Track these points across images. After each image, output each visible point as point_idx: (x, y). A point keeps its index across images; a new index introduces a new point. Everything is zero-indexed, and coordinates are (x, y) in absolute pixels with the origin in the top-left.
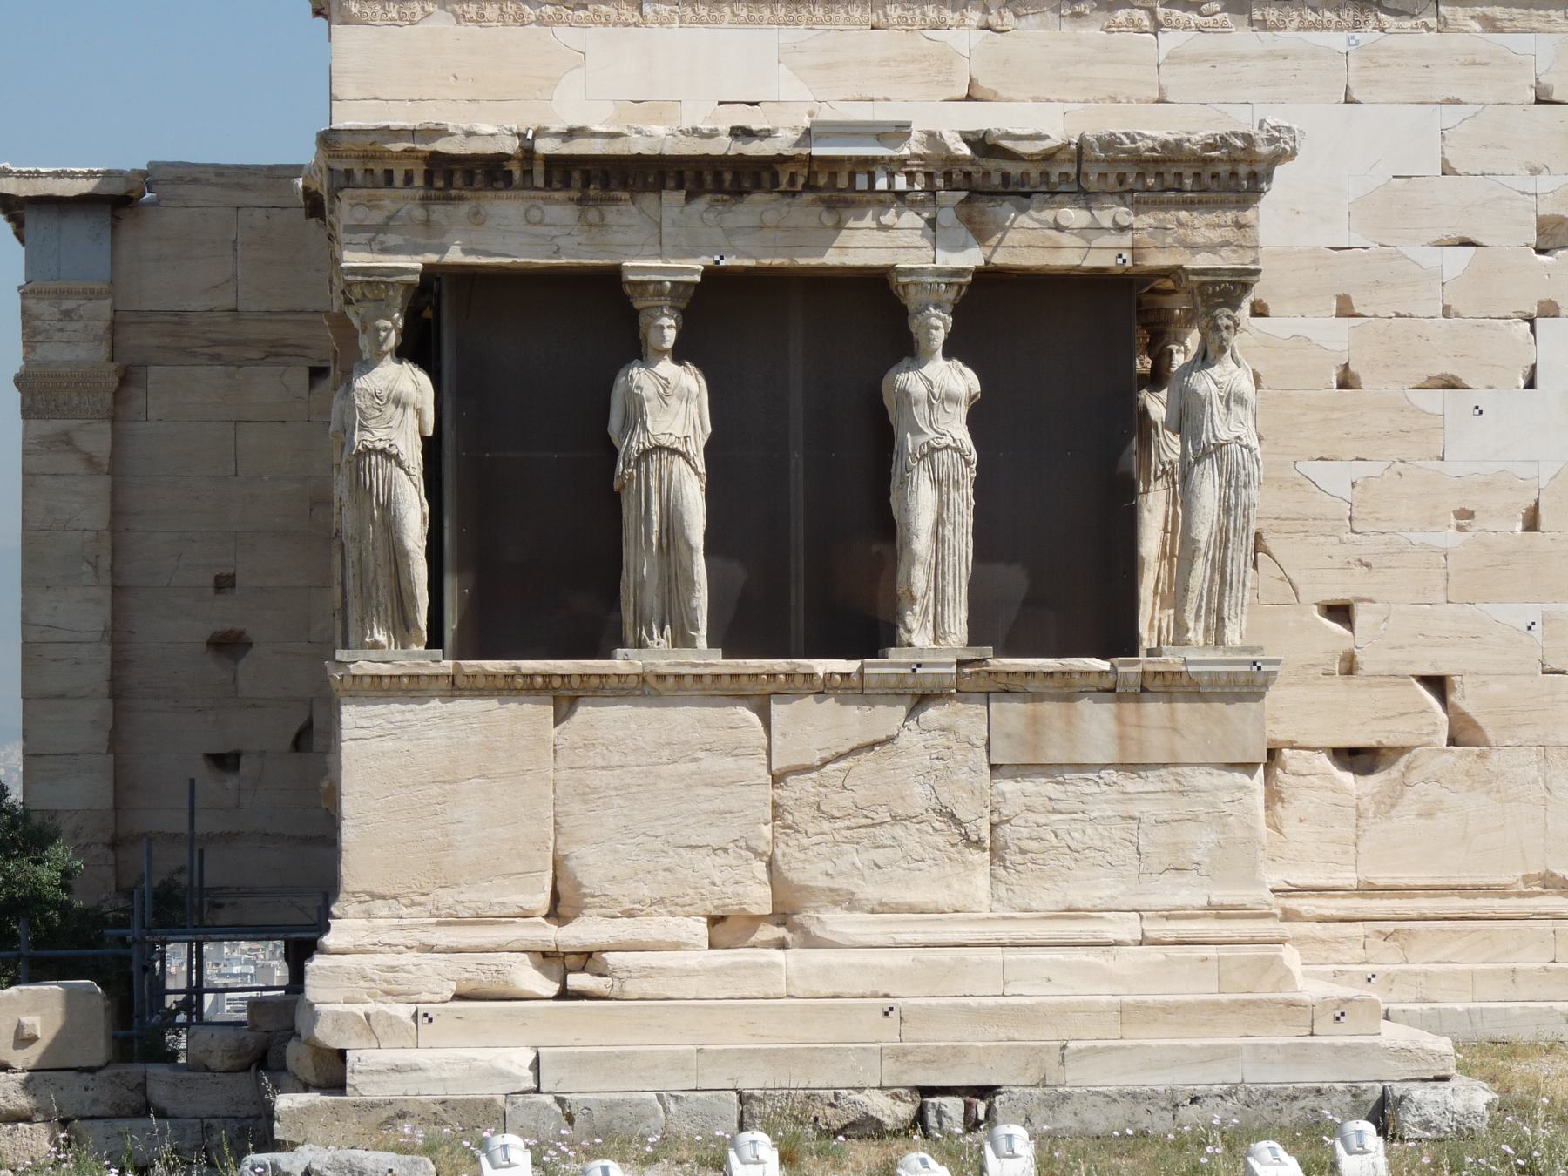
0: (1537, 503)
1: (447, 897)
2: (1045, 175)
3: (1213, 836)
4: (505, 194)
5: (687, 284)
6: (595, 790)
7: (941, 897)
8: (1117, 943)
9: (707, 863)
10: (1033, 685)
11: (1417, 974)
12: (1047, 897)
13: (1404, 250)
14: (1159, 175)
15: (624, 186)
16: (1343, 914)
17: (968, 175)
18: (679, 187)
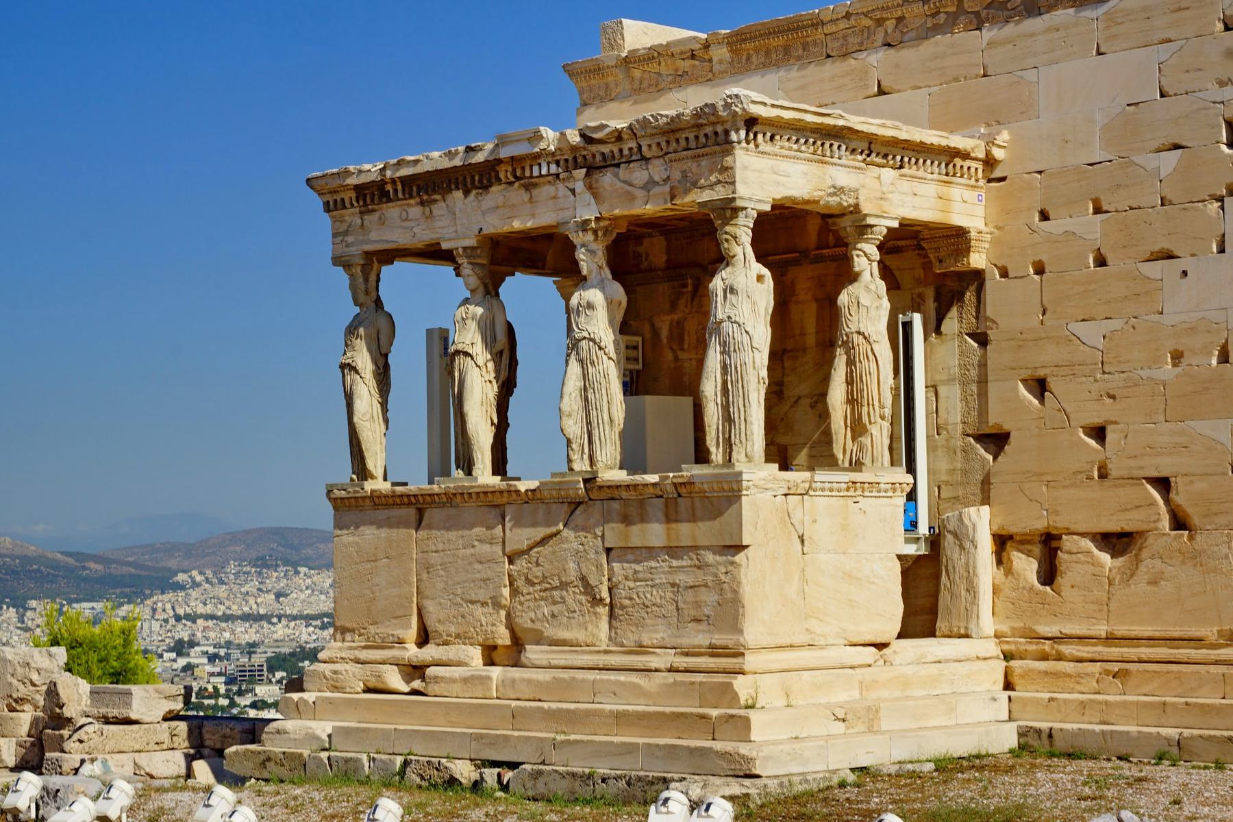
0: (1227, 340)
1: (372, 629)
2: (621, 151)
3: (716, 597)
4: (390, 204)
5: (473, 248)
6: (433, 566)
7: (581, 636)
8: (656, 670)
9: (478, 611)
10: (624, 495)
11: (1100, 703)
12: (629, 639)
13: (1134, 159)
14: (677, 141)
15: (435, 192)
16: (1089, 656)
17: (584, 157)
18: (457, 188)
